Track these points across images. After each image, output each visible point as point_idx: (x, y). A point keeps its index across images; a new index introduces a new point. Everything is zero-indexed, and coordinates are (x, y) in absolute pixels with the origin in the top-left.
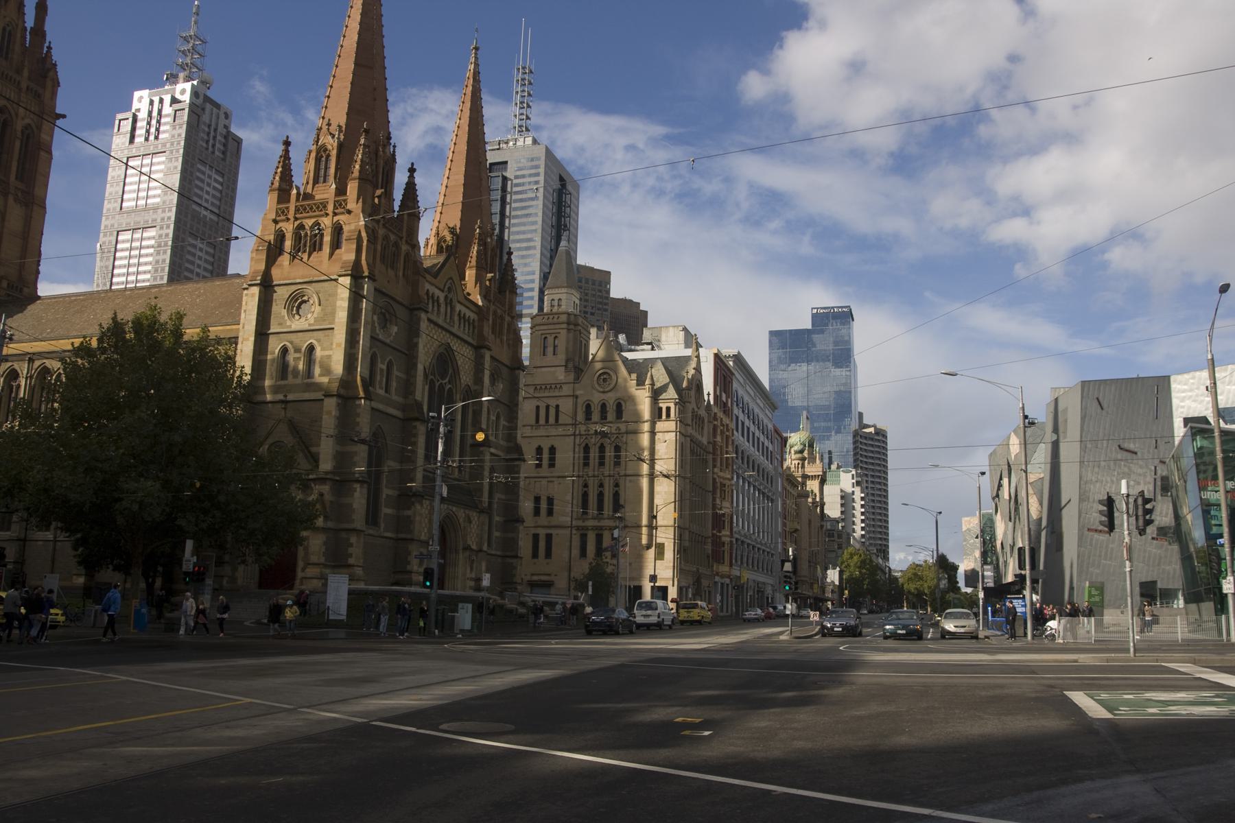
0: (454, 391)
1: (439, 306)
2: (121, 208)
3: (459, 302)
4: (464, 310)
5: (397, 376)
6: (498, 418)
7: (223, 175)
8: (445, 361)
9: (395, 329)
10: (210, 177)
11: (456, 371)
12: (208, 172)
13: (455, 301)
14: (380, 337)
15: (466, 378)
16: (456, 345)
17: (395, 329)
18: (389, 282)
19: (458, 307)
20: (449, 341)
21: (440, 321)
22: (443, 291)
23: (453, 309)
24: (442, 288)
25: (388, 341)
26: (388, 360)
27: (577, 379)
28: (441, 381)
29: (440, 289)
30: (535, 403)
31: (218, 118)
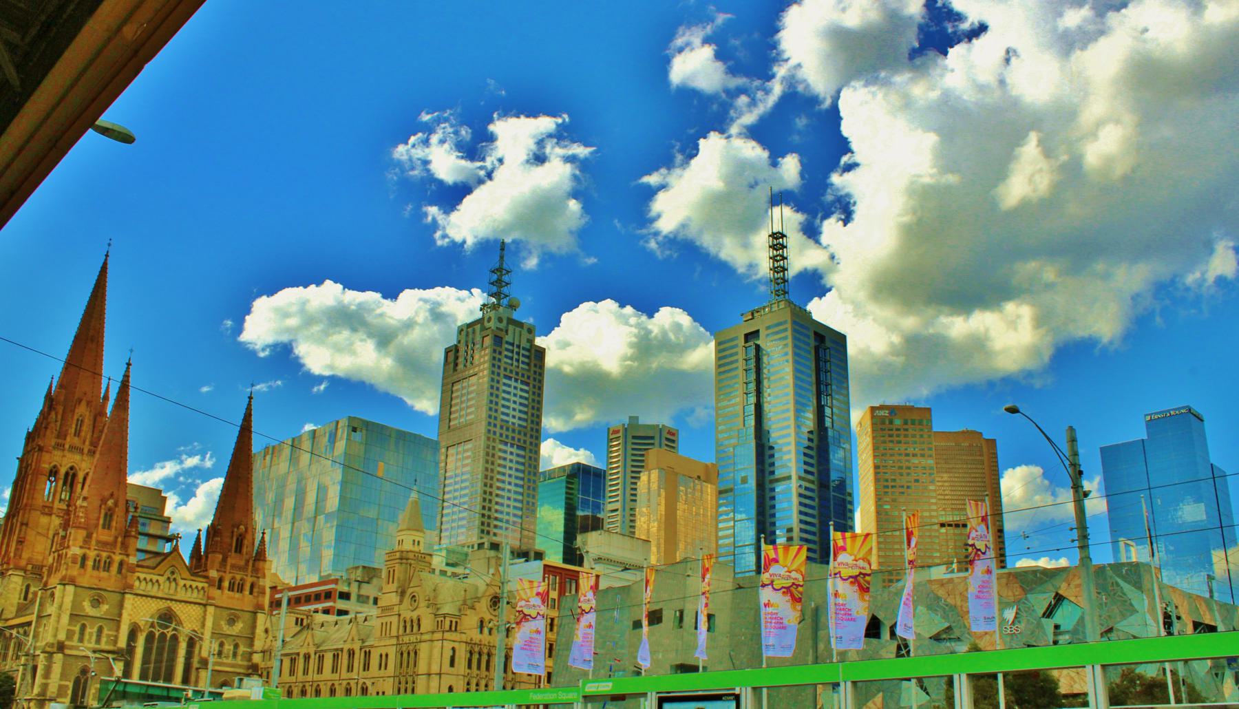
1: (159, 585)
2: (449, 427)
3: (182, 579)
4: (188, 583)
6: (236, 646)
7: (527, 384)
8: (167, 617)
10: (515, 388)
11: (180, 623)
12: (513, 383)
13: (178, 578)
14: (90, 614)
16: (178, 608)
19: (182, 583)
20: (171, 604)
21: (160, 595)
22: (162, 575)
23: (177, 584)
25: (98, 615)
27: (401, 602)
29: (159, 575)
30: (380, 620)
31: (520, 335)
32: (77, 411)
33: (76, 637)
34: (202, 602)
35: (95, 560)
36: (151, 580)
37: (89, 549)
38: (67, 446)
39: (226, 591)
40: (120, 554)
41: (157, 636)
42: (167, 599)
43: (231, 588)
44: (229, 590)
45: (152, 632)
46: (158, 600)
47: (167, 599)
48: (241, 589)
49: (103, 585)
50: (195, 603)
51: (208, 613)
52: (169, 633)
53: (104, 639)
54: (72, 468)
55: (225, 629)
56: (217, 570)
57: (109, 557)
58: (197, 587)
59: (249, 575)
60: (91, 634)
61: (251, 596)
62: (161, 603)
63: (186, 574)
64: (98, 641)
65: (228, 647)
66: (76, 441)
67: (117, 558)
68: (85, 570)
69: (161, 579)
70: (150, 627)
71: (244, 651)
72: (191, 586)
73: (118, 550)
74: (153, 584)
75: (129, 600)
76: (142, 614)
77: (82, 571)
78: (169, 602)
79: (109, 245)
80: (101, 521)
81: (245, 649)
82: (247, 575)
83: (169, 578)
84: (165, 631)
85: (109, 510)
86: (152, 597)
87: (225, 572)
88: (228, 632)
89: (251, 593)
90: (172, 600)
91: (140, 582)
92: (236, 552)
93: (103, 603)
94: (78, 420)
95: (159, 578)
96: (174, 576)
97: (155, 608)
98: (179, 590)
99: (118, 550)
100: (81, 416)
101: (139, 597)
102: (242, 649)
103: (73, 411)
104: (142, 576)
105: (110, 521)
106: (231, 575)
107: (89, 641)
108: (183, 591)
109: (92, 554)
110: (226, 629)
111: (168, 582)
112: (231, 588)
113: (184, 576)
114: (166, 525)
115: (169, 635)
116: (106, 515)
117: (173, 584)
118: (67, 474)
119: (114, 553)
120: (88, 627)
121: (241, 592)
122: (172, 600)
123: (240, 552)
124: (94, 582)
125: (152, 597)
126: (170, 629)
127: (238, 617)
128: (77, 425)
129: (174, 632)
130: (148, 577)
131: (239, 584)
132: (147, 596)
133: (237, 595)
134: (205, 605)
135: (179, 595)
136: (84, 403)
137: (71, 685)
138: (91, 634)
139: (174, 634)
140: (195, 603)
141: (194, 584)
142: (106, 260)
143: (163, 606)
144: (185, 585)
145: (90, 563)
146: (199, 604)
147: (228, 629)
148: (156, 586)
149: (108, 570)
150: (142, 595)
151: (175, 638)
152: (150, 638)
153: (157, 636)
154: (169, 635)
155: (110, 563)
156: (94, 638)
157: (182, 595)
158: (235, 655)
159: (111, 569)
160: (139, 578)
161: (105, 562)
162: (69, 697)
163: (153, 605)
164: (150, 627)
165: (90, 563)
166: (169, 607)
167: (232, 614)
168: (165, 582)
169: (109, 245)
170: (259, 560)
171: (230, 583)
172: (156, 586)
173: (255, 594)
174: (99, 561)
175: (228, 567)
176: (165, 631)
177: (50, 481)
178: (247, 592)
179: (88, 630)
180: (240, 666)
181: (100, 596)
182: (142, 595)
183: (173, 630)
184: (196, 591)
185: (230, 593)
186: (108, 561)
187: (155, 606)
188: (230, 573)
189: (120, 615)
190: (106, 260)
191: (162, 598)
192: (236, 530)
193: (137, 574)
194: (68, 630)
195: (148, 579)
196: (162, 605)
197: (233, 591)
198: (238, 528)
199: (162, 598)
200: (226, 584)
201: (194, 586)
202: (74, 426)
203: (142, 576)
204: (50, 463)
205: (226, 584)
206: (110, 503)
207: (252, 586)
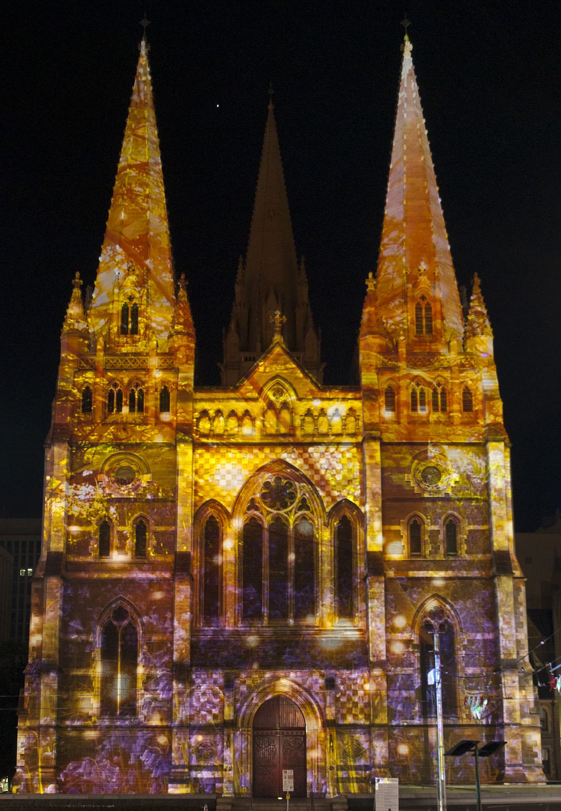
3: (300, 399)
21: (257, 438)
28: (275, 512)
62: (262, 456)
70: (249, 509)
71: (470, 531)
84: (282, 512)
104: (211, 407)
113: (301, 396)
144: (309, 413)
145: (100, 399)
156: (130, 543)
158: (452, 546)
160: (204, 413)
168: (264, 414)
180: (470, 565)
193: (200, 406)
203: (211, 407)
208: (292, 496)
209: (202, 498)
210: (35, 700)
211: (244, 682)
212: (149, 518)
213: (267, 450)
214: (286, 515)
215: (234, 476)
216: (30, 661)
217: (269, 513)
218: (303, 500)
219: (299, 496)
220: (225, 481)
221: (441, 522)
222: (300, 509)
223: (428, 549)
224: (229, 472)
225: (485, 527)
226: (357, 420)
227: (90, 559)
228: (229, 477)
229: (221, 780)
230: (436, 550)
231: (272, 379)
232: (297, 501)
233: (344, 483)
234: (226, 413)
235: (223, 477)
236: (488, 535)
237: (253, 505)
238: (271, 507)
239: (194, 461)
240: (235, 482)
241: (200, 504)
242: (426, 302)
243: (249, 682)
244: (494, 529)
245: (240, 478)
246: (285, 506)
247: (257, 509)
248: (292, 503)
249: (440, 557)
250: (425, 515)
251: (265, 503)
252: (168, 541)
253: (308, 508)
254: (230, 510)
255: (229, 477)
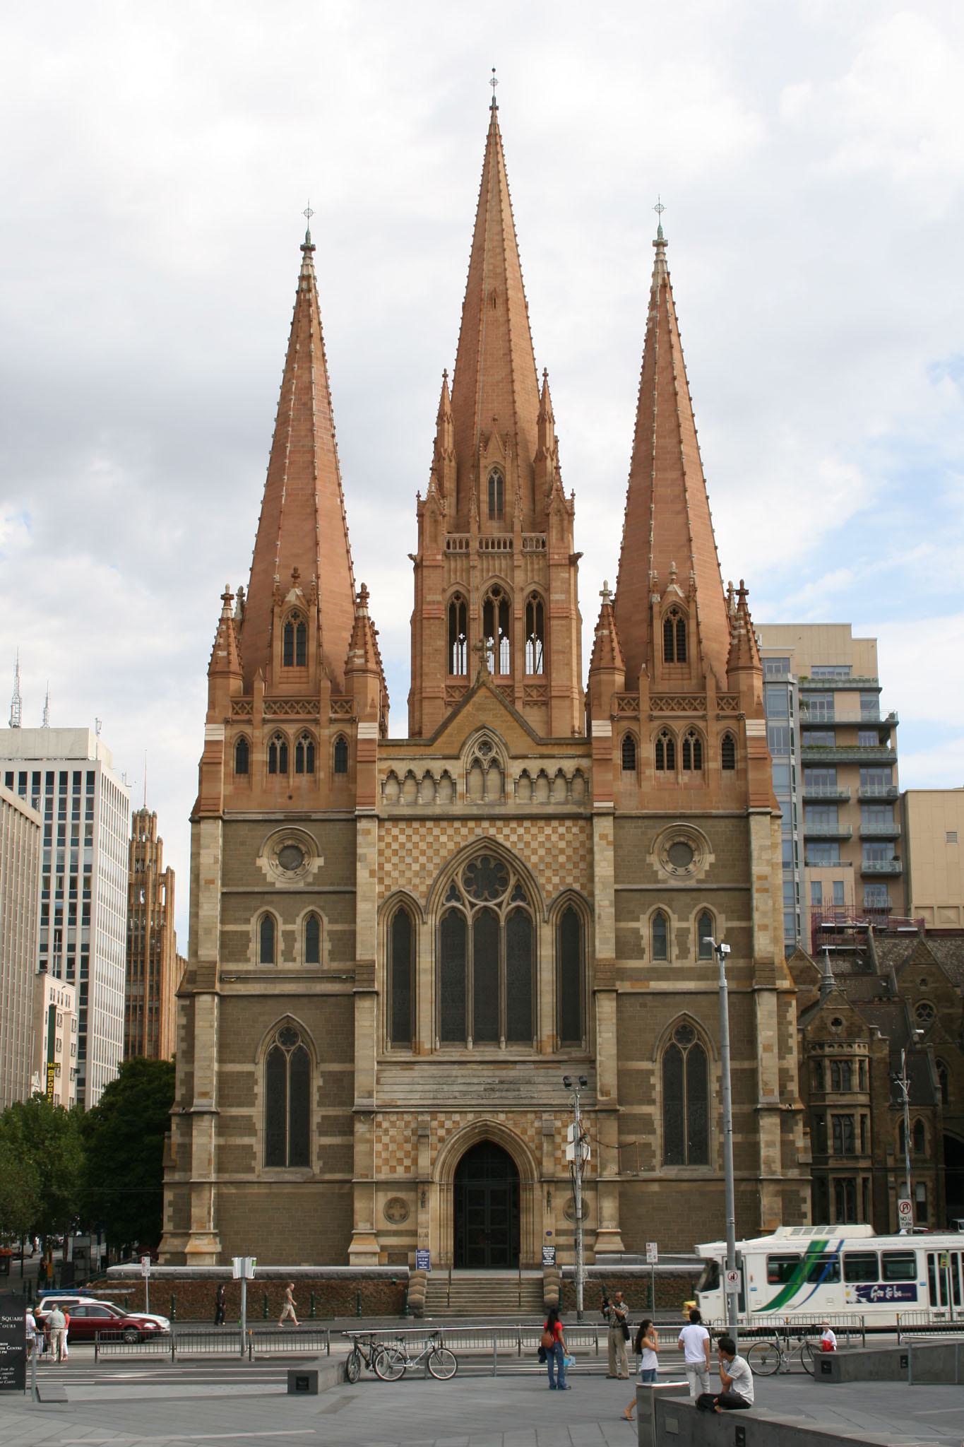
0: (531, 911)
1: (454, 784)
3: (515, 758)
4: (534, 766)
5: (330, 933)
9: (319, 862)
13: (503, 759)
14: (280, 885)
15: (550, 884)
16: (510, 837)
17: (319, 862)
18: (290, 798)
19: (515, 768)
20: (492, 831)
21: (458, 809)
22: (457, 758)
23: (503, 775)
24: (454, 752)
25: (301, 886)
26: (302, 914)
28: (483, 904)
29: (446, 758)
32: (483, 462)
33: (255, 947)
34: (581, 810)
35: (273, 749)
36: (428, 774)
37: (249, 722)
38: (474, 545)
39: (650, 772)
40: (332, 721)
41: (470, 921)
42: (478, 819)
43: (665, 760)
44: (659, 767)
45: (454, 909)
46: (457, 824)
47: (478, 819)
48: (695, 759)
49: (302, 806)
50: (561, 818)
51: (596, 838)
52: (504, 905)
53: (325, 946)
54: (496, 590)
55: (661, 874)
56: (612, 718)
57: (306, 734)
58: (560, 772)
59: (712, 711)
60: (289, 936)
61: (727, 773)
62: (464, 831)
63: (521, 743)
64: (312, 953)
65: (682, 923)
66: (494, 530)
67: (326, 734)
68: (250, 777)
69: (456, 768)
70: (448, 899)
72: (543, 773)
73: (327, 713)
74: (435, 784)
75: (369, 840)
76: (416, 867)
77: (242, 779)
78: (486, 824)
79: (494, 83)
80: (279, 647)
81: (730, 924)
82: (703, 718)
83: (477, 762)
84: (491, 904)
85: (295, 616)
86: (437, 819)
87: (636, 719)
88: (673, 884)
89: (728, 763)
90: (493, 818)
91: (400, 784)
92: (668, 658)
93: (308, 853)
94: (491, 481)
95: (449, 765)
96: (493, 754)
97: (451, 846)
98: (510, 787)
99: (327, 713)
100: (496, 470)
101: (402, 825)
102: (722, 923)
103: (476, 466)
104: (401, 768)
105: (303, 643)
106: (656, 723)
107: (289, 956)
108: (524, 792)
109: (259, 736)
110: (665, 873)
111: (476, 772)
112: (665, 760)
113: (514, 752)
114: (869, 697)
115: (503, 914)
116: (288, 630)
117: (493, 777)
118: (488, 607)
119: (316, 721)
120: (280, 920)
121: (698, 767)
122: (493, 818)
123: (683, 658)
124: (277, 805)
125: (437, 819)
126: (505, 897)
127: (697, 838)
128: (491, 494)
129: (514, 905)
130: (419, 768)
131: (686, 745)
132: (423, 819)
133: (685, 777)
134: (589, 818)
135: (510, 801)
136: (495, 443)
137: (260, 1070)
138: (289, 936)
139: (518, 907)
140: (561, 818)
141: (552, 767)
142: (494, 117)
143: (472, 839)
144: (525, 773)
145: (259, 757)
146: (575, 817)
147: (673, 873)
148: (445, 791)
149: (311, 769)
150: (409, 819)
151: (523, 923)
152: (452, 926)
153: (470, 921)
154: (503, 914)
155: (311, 748)
156: (300, 946)
157: (518, 801)
159: (317, 763)
160: (392, 774)
161: (300, 748)
162: (261, 1101)
163: (443, 839)
164: (448, 899)
165: (259, 757)
166: (492, 839)
167: (679, 831)
169: (494, 83)
170: (737, 669)
171: (659, 747)
172: (445, 791)
173: (739, 765)
174: (284, 749)
175: (645, 705)
176: (491, 904)
177: (532, 640)
178: (714, 762)
179: (281, 927)
181: (294, 834)
182: (409, 819)
183: (514, 899)
184: (560, 782)
185: (666, 774)
186: (305, 744)
187: (449, 840)
188: (651, 718)
189: (352, 878)
190: (494, 117)
191: (464, 819)
192: (656, 598)
194: (223, 933)
195: (419, 774)
196: (467, 834)
197: (671, 766)
198: (663, 594)
199: (464, 819)
200: (647, 751)
201: (552, 772)
202: (484, 497)
204: (444, 590)
205: (647, 751)
206: (294, 595)
207: (729, 745)
208: (505, 882)
209: (388, 887)
210: (186, 1149)
211: (442, 1126)
212: (321, 913)
213: (471, 824)
214: (496, 908)
215: (430, 859)
216: (178, 1097)
217: (473, 905)
218: (518, 887)
219: (512, 881)
220: (418, 865)
221: (692, 917)
222: (514, 899)
223: (674, 951)
224: (423, 853)
225: (743, 924)
226: (586, 783)
227: (250, 967)
228: (423, 860)
229: (414, 1248)
230: (684, 953)
231: (477, 730)
232: (509, 889)
233: (570, 866)
234: (419, 774)
235: (416, 860)
236: (748, 933)
237: (454, 894)
238: (476, 897)
239: (381, 838)
240: (430, 866)
241: (388, 894)
242: (677, 618)
243: (448, 1124)
244: (756, 928)
245: (437, 860)
246: (495, 895)
247: (459, 899)
248: (504, 892)
249: (691, 962)
250: (670, 907)
251: (468, 892)
252: (347, 942)
253: (524, 899)
254: (422, 902)
255: (423, 860)
